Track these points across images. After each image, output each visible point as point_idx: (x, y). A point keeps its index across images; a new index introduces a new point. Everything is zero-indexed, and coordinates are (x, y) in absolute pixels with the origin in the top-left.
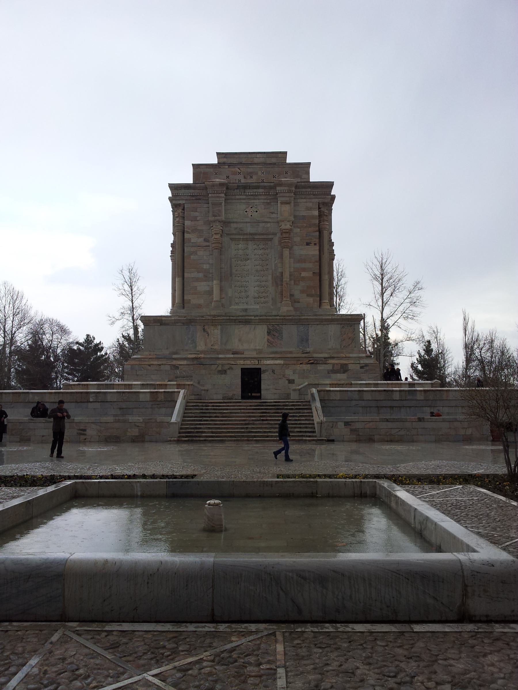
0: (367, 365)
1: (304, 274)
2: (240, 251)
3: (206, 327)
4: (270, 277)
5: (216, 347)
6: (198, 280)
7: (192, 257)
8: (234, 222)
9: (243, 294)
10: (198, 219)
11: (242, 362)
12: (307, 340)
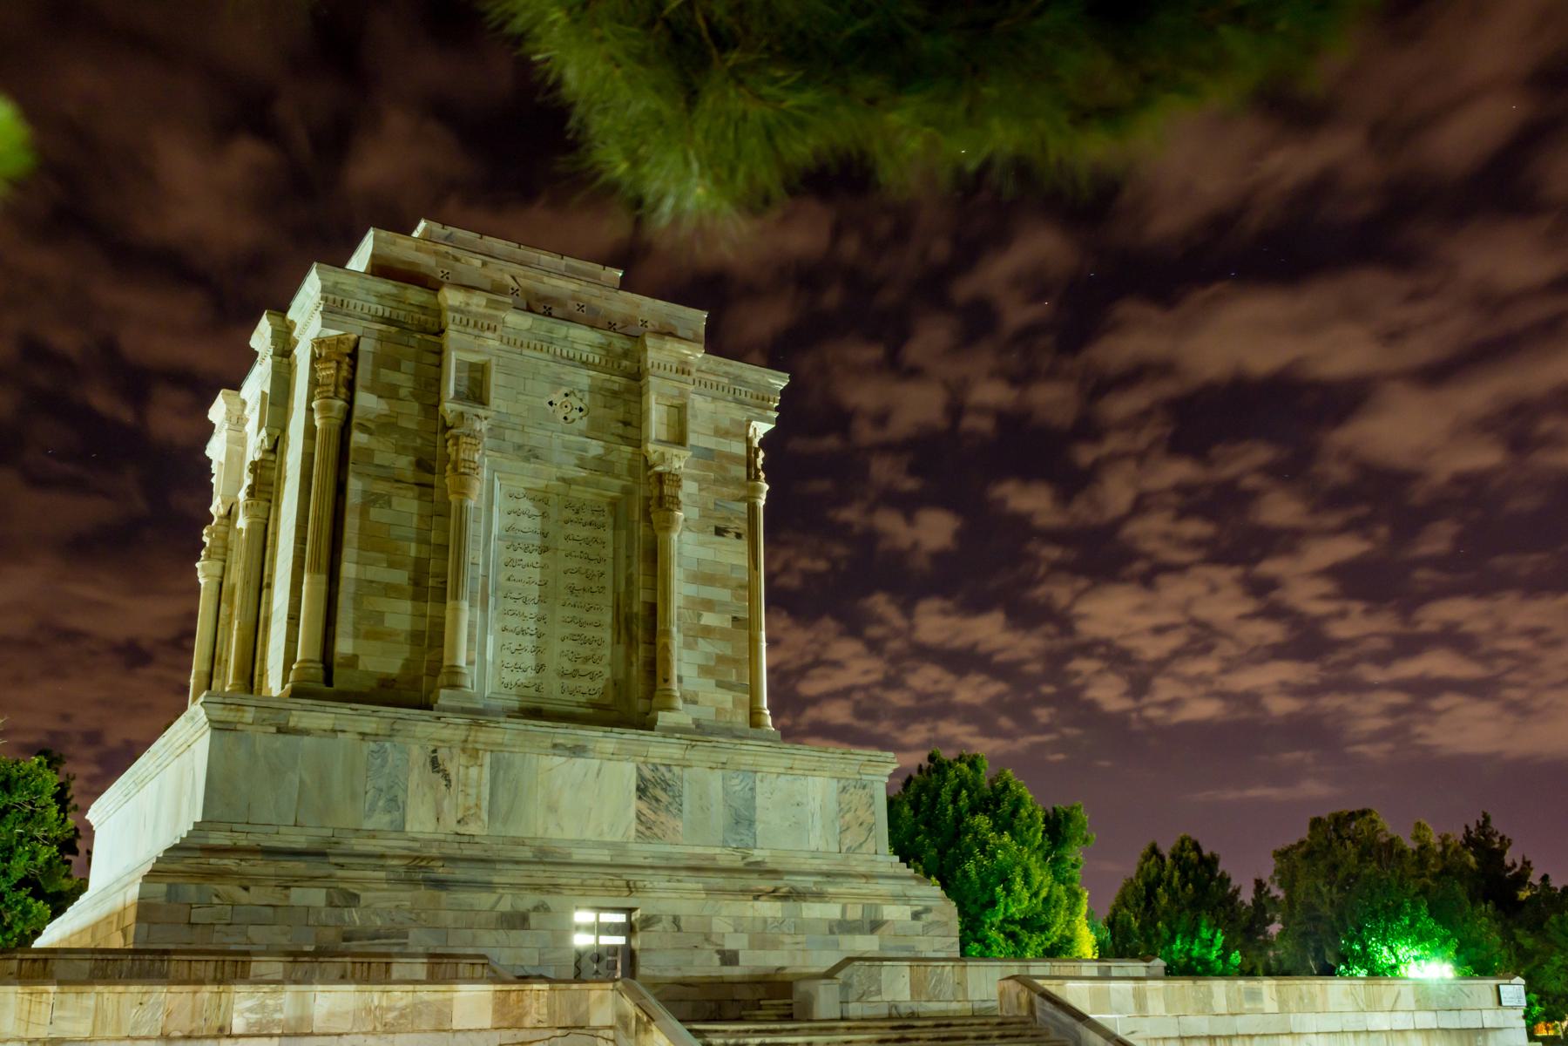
1: (709, 619)
3: (442, 754)
4: (607, 618)
5: (472, 828)
10: (403, 392)
12: (751, 823)
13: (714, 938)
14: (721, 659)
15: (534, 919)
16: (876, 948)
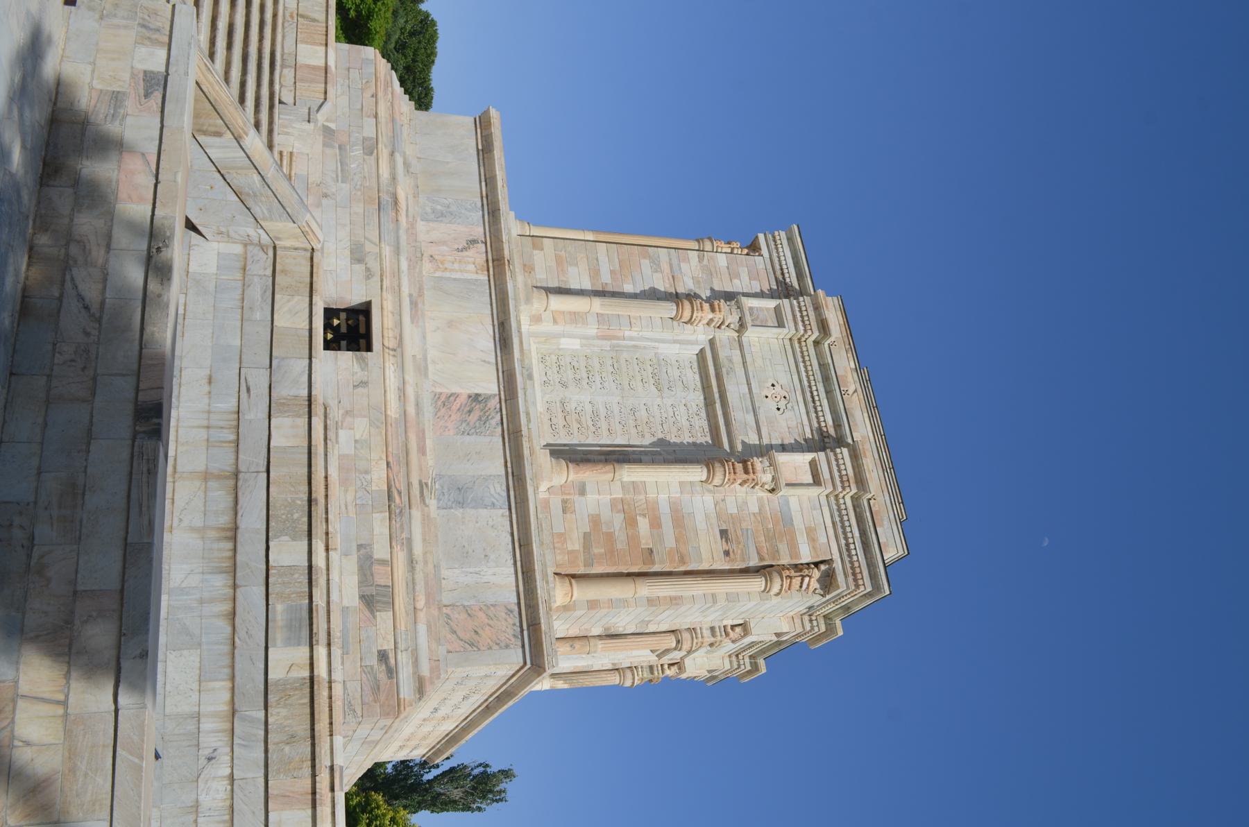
0: (391, 672)
2: (677, 373)
7: (647, 261)
8: (743, 356)
9: (570, 373)
10: (736, 281)
11: (389, 305)
12: (461, 504)
13: (348, 419)
14: (610, 537)
15: (359, 268)
16: (346, 603)
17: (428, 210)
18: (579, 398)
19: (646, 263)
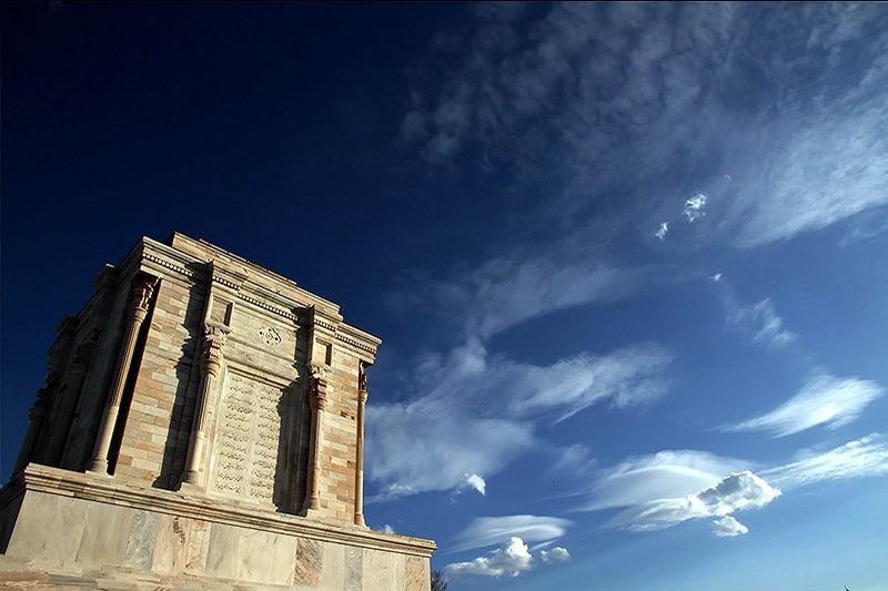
1: (335, 460)
5: (196, 571)
6: (156, 421)
12: (360, 578)
14: (340, 484)
17: (140, 560)
18: (250, 471)
19: (155, 375)
